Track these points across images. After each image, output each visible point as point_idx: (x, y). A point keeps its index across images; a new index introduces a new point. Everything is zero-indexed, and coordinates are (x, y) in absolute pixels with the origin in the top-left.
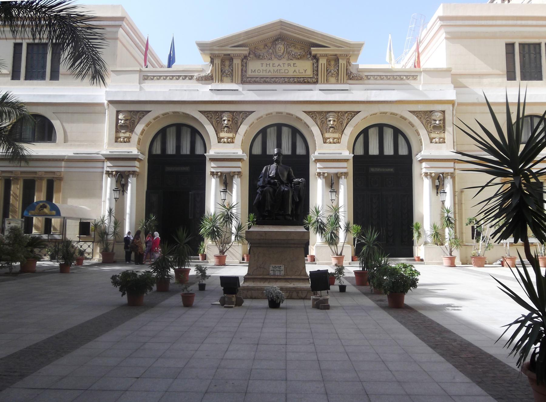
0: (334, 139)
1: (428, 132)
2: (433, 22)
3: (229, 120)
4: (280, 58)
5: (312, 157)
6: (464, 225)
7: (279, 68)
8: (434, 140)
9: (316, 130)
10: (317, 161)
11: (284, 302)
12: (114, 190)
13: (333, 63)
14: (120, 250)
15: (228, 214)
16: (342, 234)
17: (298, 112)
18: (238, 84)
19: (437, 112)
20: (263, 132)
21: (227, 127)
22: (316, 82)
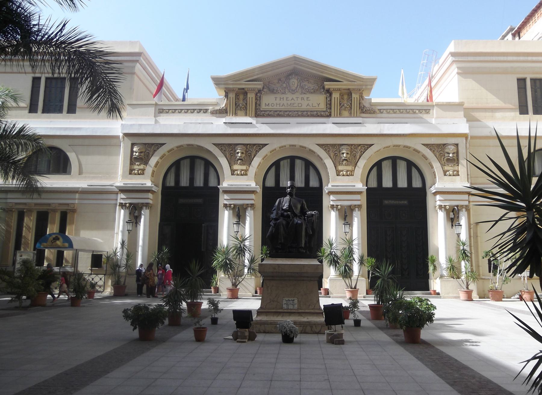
0: (347, 171)
1: (441, 164)
2: (445, 58)
3: (242, 153)
4: (293, 92)
5: (326, 190)
6: (480, 258)
7: (293, 102)
9: (329, 163)
10: (330, 193)
11: (298, 336)
12: (127, 222)
13: (346, 97)
14: (132, 283)
15: (241, 247)
16: (356, 267)
17: (311, 144)
18: (251, 117)
19: (450, 145)
20: (277, 165)
21: (241, 159)
22: (329, 116)
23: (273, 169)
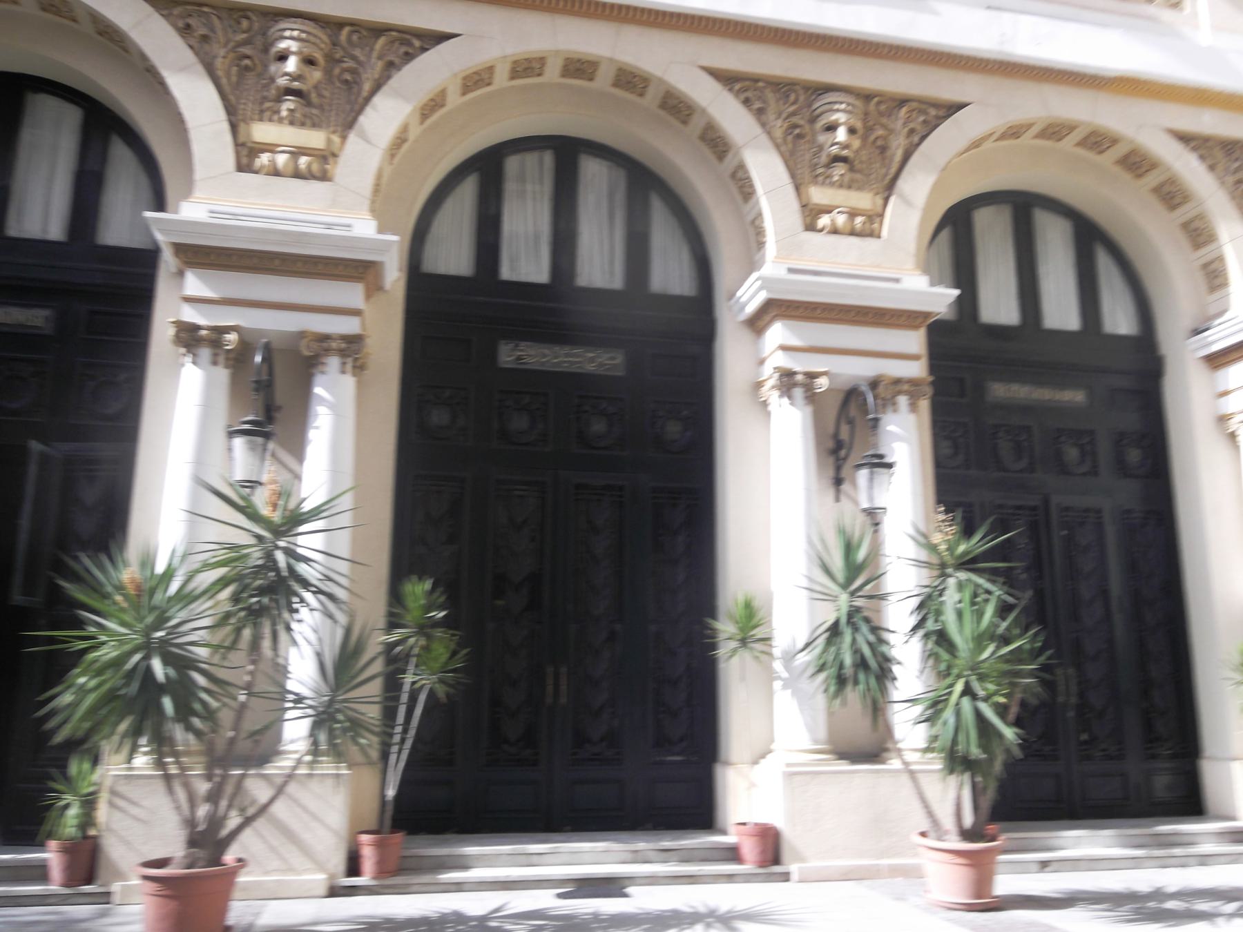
0: (853, 214)
3: (309, 61)
20: (487, 168)
23: (468, 191)
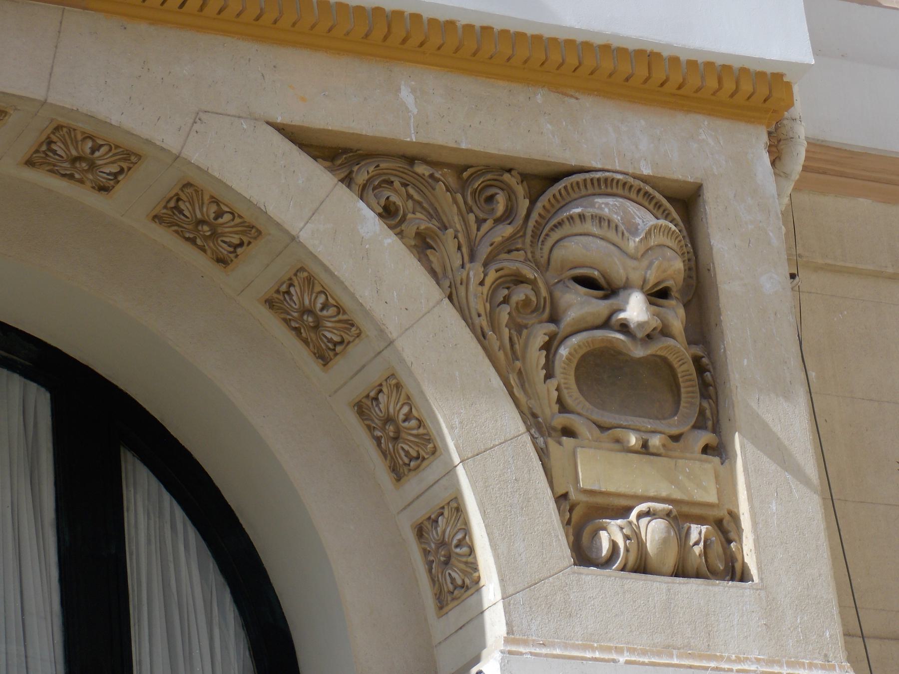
1: (532, 419)
8: (611, 534)
